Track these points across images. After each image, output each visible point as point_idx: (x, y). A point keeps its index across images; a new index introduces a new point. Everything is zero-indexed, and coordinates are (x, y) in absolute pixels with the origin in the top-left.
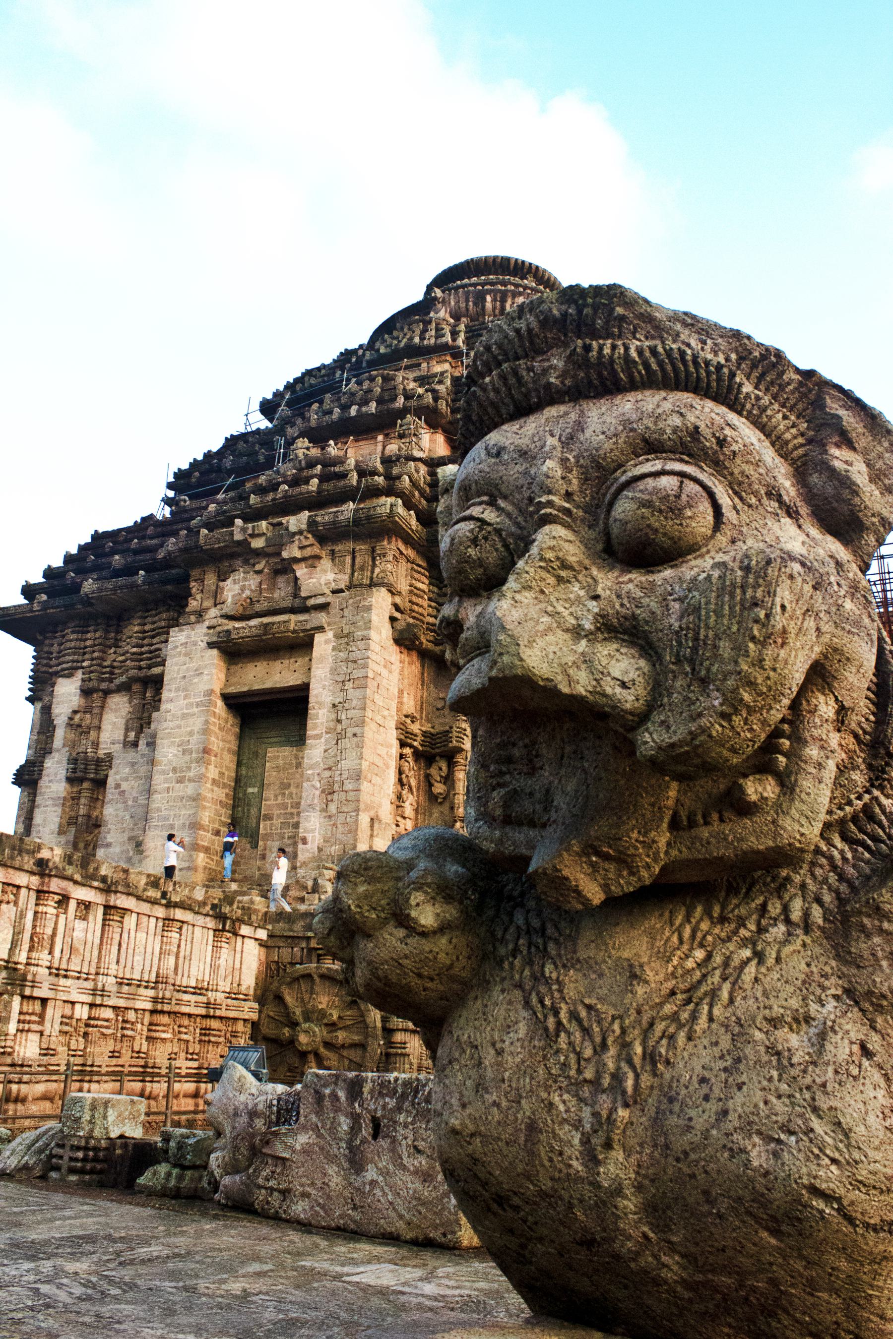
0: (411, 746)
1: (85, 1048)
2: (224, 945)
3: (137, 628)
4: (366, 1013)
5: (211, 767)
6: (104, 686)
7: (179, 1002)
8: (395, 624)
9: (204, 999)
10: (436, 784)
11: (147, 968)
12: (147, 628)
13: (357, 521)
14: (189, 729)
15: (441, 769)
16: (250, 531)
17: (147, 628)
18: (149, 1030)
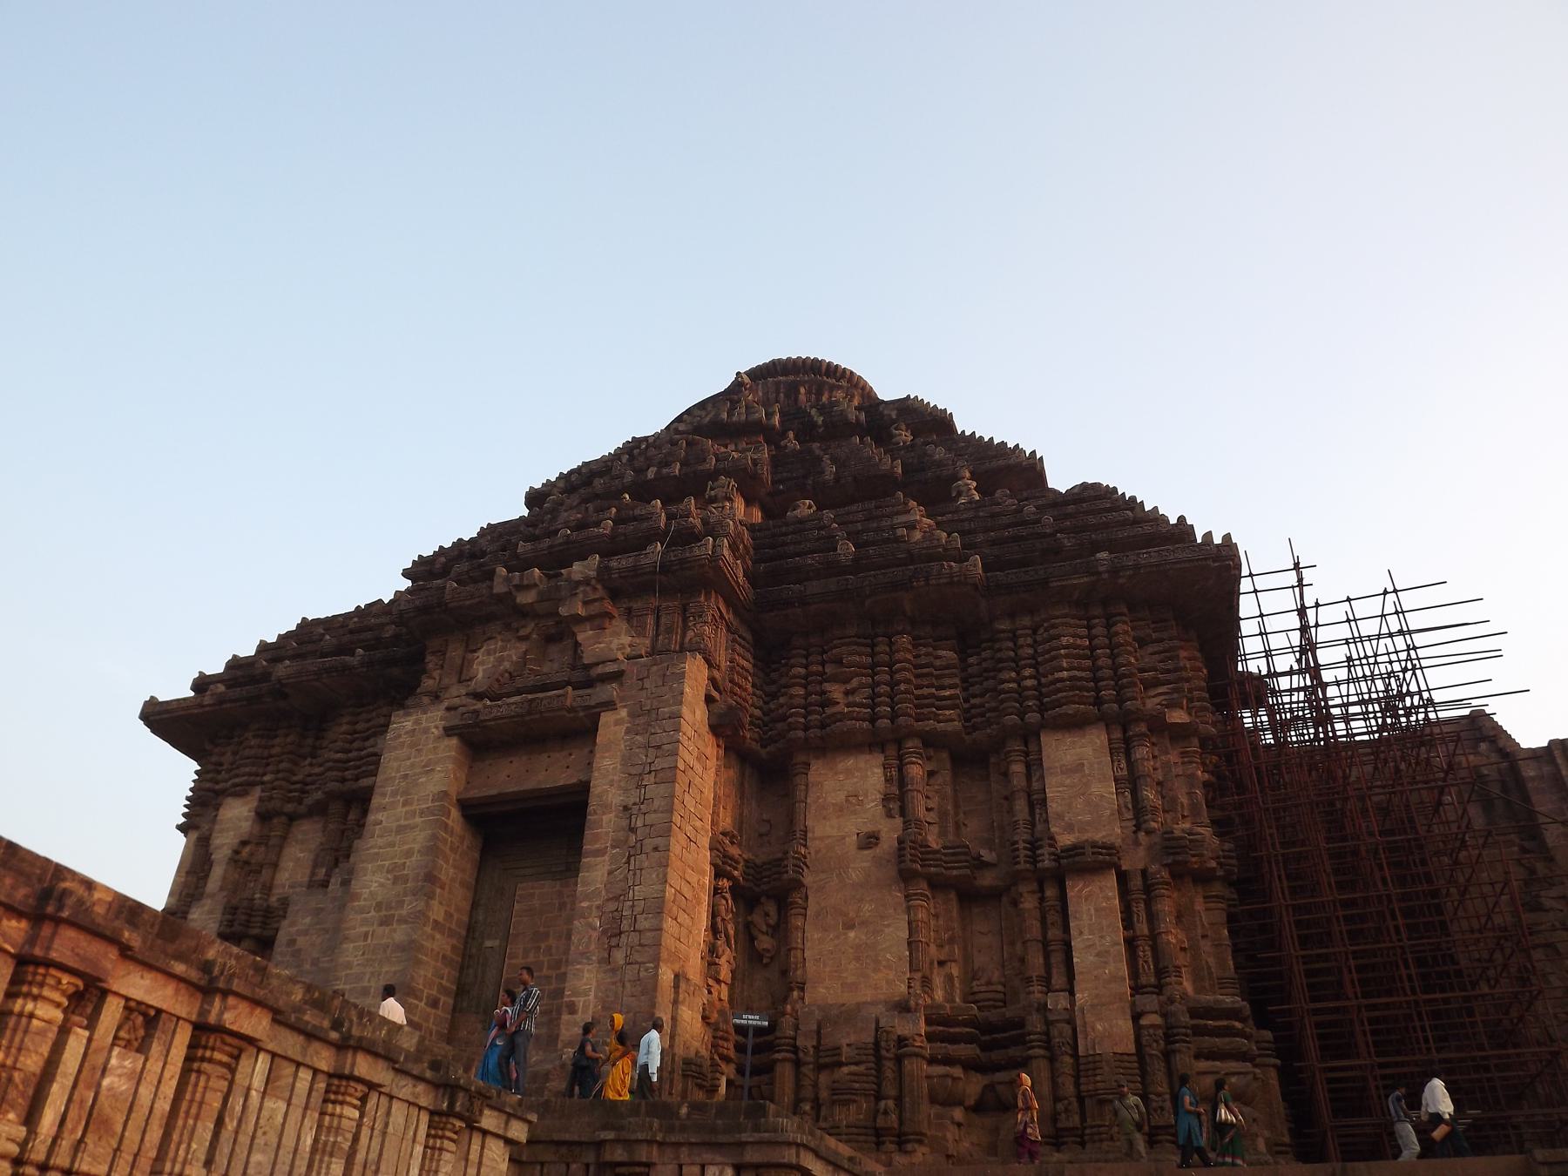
0: (730, 877)
2: (447, 1144)
3: (344, 728)
5: (435, 903)
6: (289, 808)
12: (359, 727)
13: (665, 568)
14: (406, 847)
15: (767, 915)
17: (359, 727)
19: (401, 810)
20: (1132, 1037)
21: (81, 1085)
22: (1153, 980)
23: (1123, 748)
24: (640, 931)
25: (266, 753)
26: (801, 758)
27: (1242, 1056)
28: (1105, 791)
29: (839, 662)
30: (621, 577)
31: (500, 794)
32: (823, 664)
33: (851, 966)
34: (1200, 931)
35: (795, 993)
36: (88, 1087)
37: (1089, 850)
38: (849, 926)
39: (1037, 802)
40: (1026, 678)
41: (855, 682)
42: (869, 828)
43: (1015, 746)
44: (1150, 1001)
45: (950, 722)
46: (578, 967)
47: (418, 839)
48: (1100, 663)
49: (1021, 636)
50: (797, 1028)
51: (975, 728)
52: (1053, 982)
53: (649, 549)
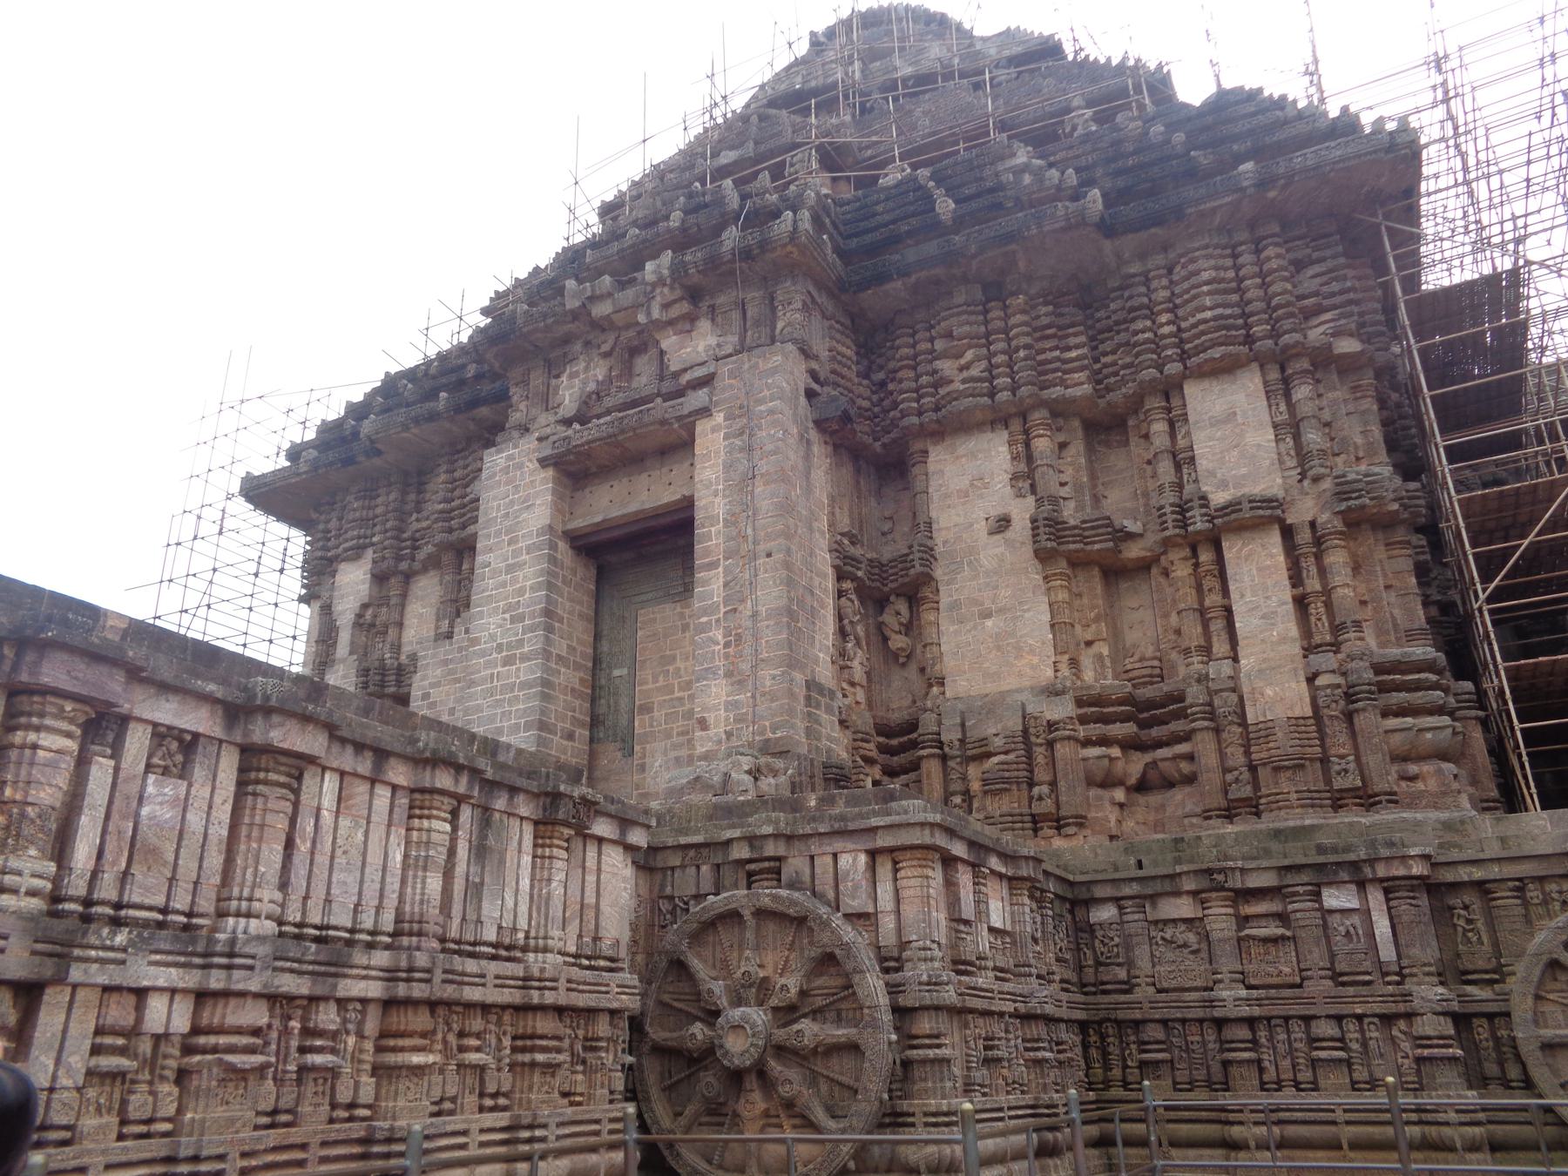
0: (854, 579)
1: (180, 1111)
3: (443, 477)
4: (856, 979)
6: (404, 566)
7: (455, 977)
8: (814, 401)
9: (517, 969)
10: (894, 636)
11: (370, 900)
12: (457, 474)
13: (746, 254)
15: (898, 613)
16: (589, 294)
17: (457, 474)
18: (379, 1049)
20: (1308, 700)
21: (115, 816)
22: (1328, 638)
25: (371, 514)
26: (917, 446)
27: (1439, 710)
29: (949, 335)
32: (932, 340)
34: (1381, 582)
35: (935, 690)
36: (124, 817)
37: (1246, 506)
38: (988, 615)
39: (1183, 460)
40: (1162, 325)
41: (969, 355)
42: (996, 512)
43: (1154, 402)
44: (1327, 660)
45: (1080, 388)
48: (1249, 295)
49: (1154, 278)
50: (940, 724)
51: (1108, 389)
52: (1215, 650)
53: (725, 235)
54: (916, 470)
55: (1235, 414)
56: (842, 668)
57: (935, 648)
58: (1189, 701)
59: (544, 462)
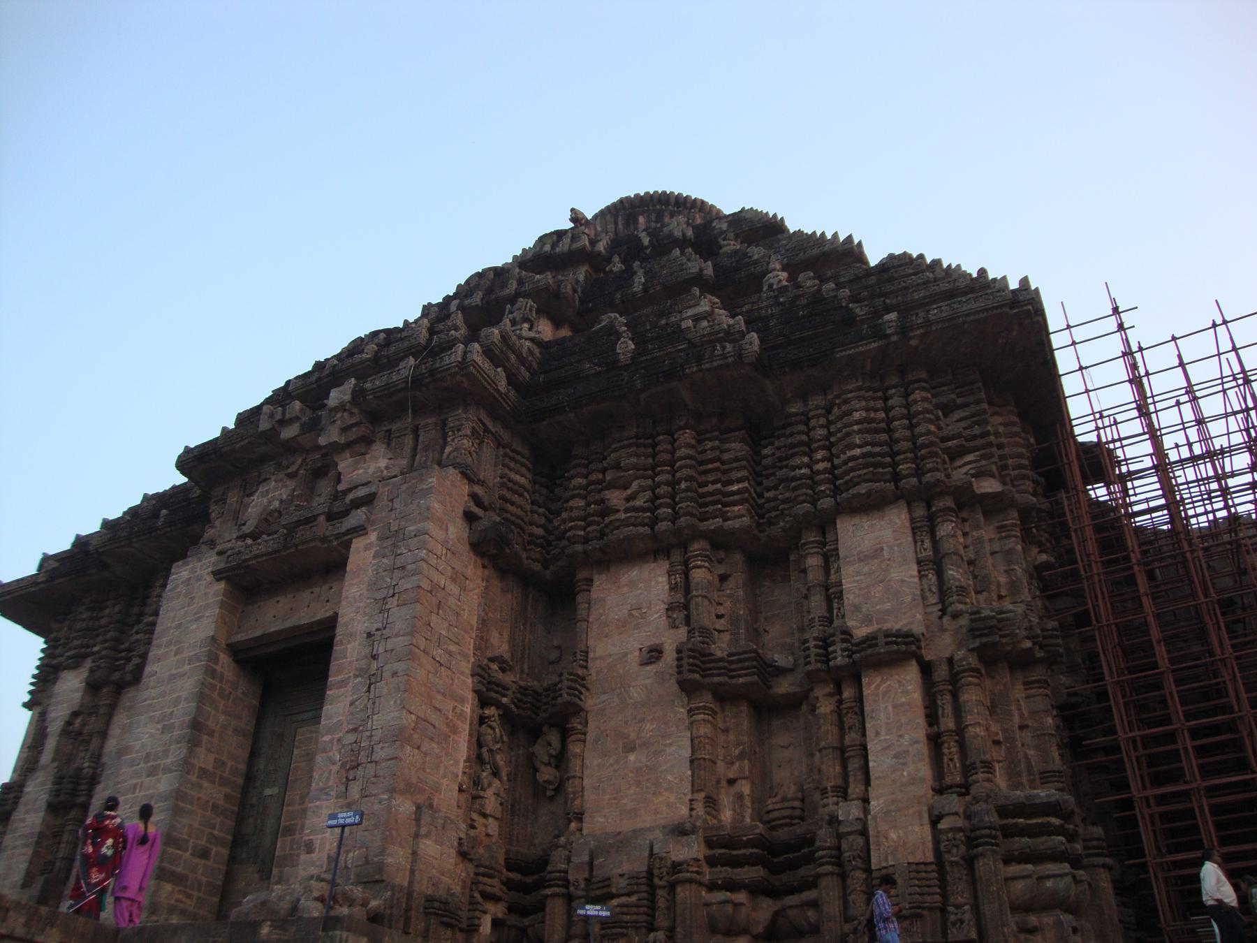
0: (499, 706)
5: (201, 751)
6: (116, 676)
10: (543, 768)
13: (417, 382)
15: (550, 745)
16: (278, 417)
19: (173, 659)
20: (930, 845)
23: (925, 527)
24: (376, 762)
26: (582, 574)
27: (1057, 857)
28: (906, 574)
29: (617, 466)
30: (375, 397)
31: (264, 635)
32: (604, 471)
33: (632, 791)
34: (1016, 720)
35: (573, 825)
37: (881, 640)
38: (630, 749)
39: (833, 595)
40: (818, 462)
41: (635, 486)
43: (811, 537)
44: (953, 802)
45: (740, 518)
46: (318, 803)
47: (188, 686)
48: (897, 435)
49: (813, 417)
50: (569, 860)
51: (771, 523)
52: (850, 791)
53: (402, 365)
54: (580, 598)
55: (882, 549)
56: (475, 798)
57: (577, 782)
58: (818, 843)
59: (218, 575)
